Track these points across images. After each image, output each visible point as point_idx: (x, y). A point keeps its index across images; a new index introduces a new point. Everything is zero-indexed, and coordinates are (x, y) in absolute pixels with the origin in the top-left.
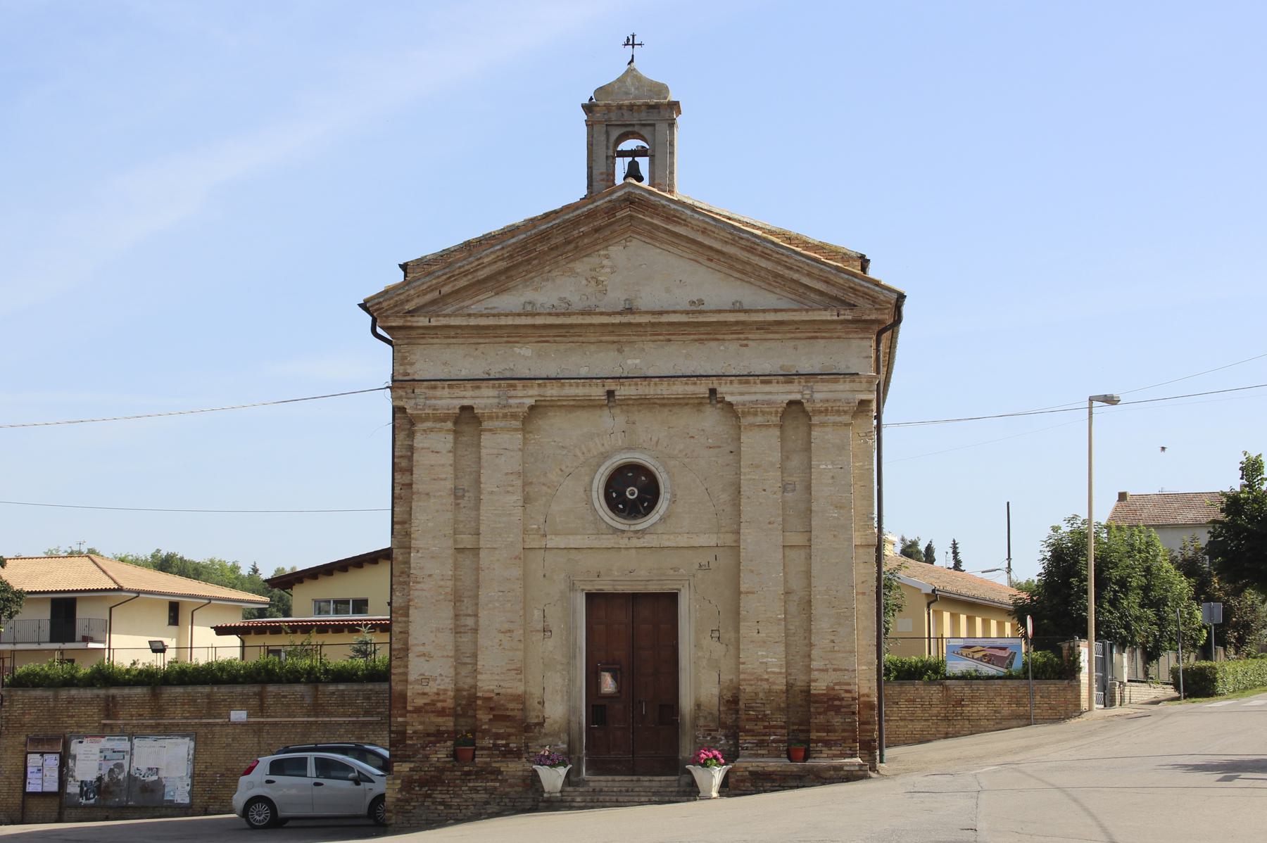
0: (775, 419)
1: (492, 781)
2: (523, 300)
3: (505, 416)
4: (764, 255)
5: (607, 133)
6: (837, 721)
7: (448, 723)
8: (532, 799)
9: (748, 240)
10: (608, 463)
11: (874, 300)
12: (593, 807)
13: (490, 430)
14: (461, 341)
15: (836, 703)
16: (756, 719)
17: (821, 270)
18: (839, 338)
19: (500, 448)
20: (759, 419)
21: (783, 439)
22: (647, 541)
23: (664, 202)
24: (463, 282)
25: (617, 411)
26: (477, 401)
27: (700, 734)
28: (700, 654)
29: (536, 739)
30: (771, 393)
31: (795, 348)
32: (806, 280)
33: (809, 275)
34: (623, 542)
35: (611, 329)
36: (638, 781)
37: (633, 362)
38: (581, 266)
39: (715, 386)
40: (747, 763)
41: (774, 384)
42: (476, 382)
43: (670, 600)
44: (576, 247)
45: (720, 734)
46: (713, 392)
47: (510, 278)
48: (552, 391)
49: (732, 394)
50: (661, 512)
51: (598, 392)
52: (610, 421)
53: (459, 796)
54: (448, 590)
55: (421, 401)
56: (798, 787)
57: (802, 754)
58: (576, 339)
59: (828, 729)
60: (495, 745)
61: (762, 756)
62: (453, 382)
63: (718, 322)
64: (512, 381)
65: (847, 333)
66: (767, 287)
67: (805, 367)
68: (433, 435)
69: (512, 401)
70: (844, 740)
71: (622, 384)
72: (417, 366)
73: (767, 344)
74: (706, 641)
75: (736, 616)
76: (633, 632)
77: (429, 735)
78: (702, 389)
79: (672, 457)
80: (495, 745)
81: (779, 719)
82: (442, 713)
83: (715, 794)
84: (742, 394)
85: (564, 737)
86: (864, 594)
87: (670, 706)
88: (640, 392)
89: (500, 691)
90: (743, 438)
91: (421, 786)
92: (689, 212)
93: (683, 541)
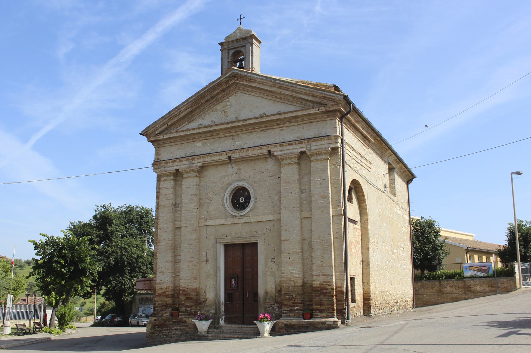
0: (296, 161)
1: (183, 326)
2: (198, 124)
3: (190, 171)
4: (287, 89)
5: (228, 53)
6: (325, 299)
7: (170, 301)
8: (194, 336)
9: (279, 83)
10: (230, 187)
11: (334, 101)
12: (215, 340)
13: (186, 178)
14: (176, 143)
15: (324, 291)
16: (289, 299)
17: (310, 91)
18: (321, 121)
19: (189, 184)
20: (288, 161)
21: (300, 169)
22: (246, 220)
23: (246, 74)
24: (175, 119)
25: (234, 165)
26: (182, 166)
27: (267, 306)
28: (267, 269)
29: (203, 308)
30: (293, 149)
31: (303, 128)
32: (305, 97)
33: (306, 94)
34: (236, 221)
35: (229, 130)
36: (242, 327)
37: (238, 143)
38: (218, 107)
39: (270, 149)
40: (284, 320)
41: (295, 145)
42: (181, 159)
43: (254, 245)
44: (217, 99)
45: (276, 306)
46: (269, 151)
47: (193, 116)
48: (208, 159)
49: (277, 151)
50: (251, 207)
51: (224, 157)
52: (231, 169)
53: (171, 332)
54: (170, 245)
55: (163, 169)
56: (306, 332)
57: (309, 316)
58: (217, 136)
59: (321, 303)
60: (186, 310)
61: (292, 317)
62: (173, 160)
63: (269, 121)
64: (193, 157)
65: (325, 118)
66: (290, 103)
67: (308, 135)
68: (166, 182)
69: (194, 165)
70: (328, 309)
71: (233, 153)
72: (162, 155)
73: (291, 128)
74: (270, 264)
75: (280, 252)
76: (241, 259)
77: (163, 306)
78: (265, 151)
79: (255, 182)
80: (186, 310)
81: (299, 299)
82: (167, 296)
83: (266, 334)
84: (281, 151)
85: (213, 307)
86: (337, 238)
87: (256, 294)
88: (240, 155)
89: (189, 287)
90: (282, 170)
91: (158, 328)
92: (255, 76)
93: (259, 219)
